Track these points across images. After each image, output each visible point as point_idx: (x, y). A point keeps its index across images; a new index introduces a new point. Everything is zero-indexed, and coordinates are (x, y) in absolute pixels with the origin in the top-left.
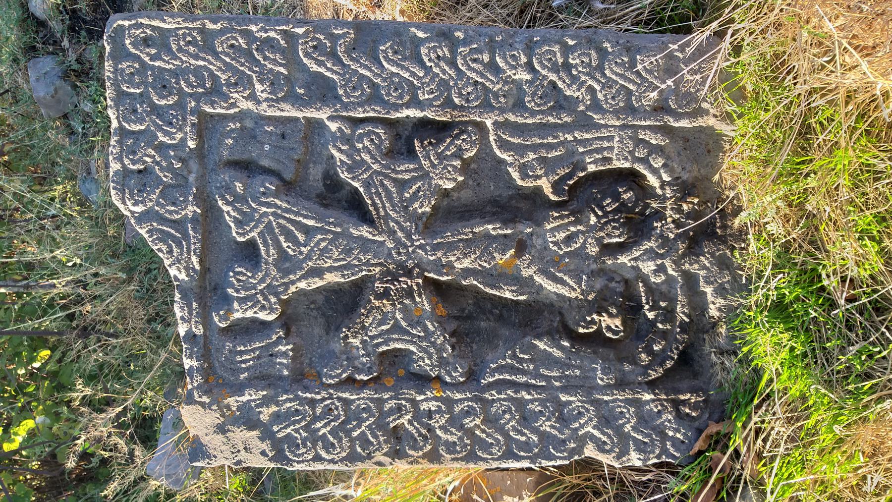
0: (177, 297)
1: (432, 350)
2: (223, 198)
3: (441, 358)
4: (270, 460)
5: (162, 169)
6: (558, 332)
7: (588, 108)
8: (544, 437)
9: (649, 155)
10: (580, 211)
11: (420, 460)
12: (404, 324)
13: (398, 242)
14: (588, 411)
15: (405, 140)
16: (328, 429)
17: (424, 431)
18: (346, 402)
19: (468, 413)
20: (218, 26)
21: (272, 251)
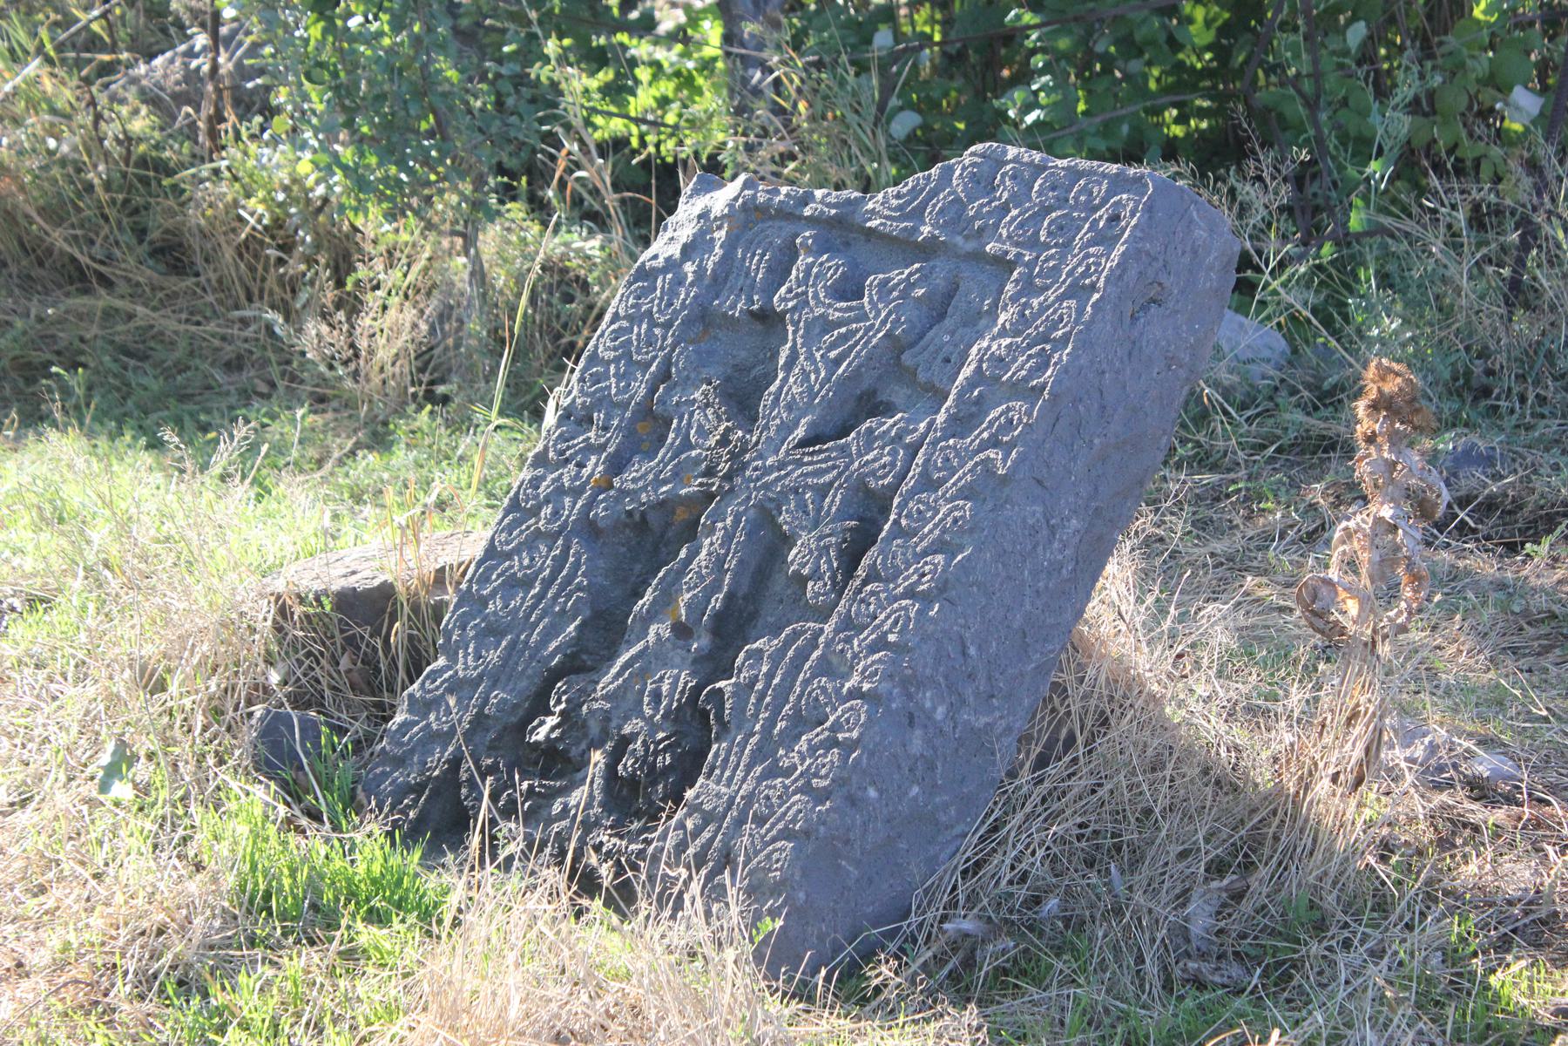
1: (641, 484)
2: (917, 271)
4: (643, 264)
5: (982, 206)
6: (574, 656)
8: (484, 602)
10: (676, 720)
13: (767, 471)
14: (475, 668)
19: (556, 514)
20: (1089, 309)
21: (837, 314)
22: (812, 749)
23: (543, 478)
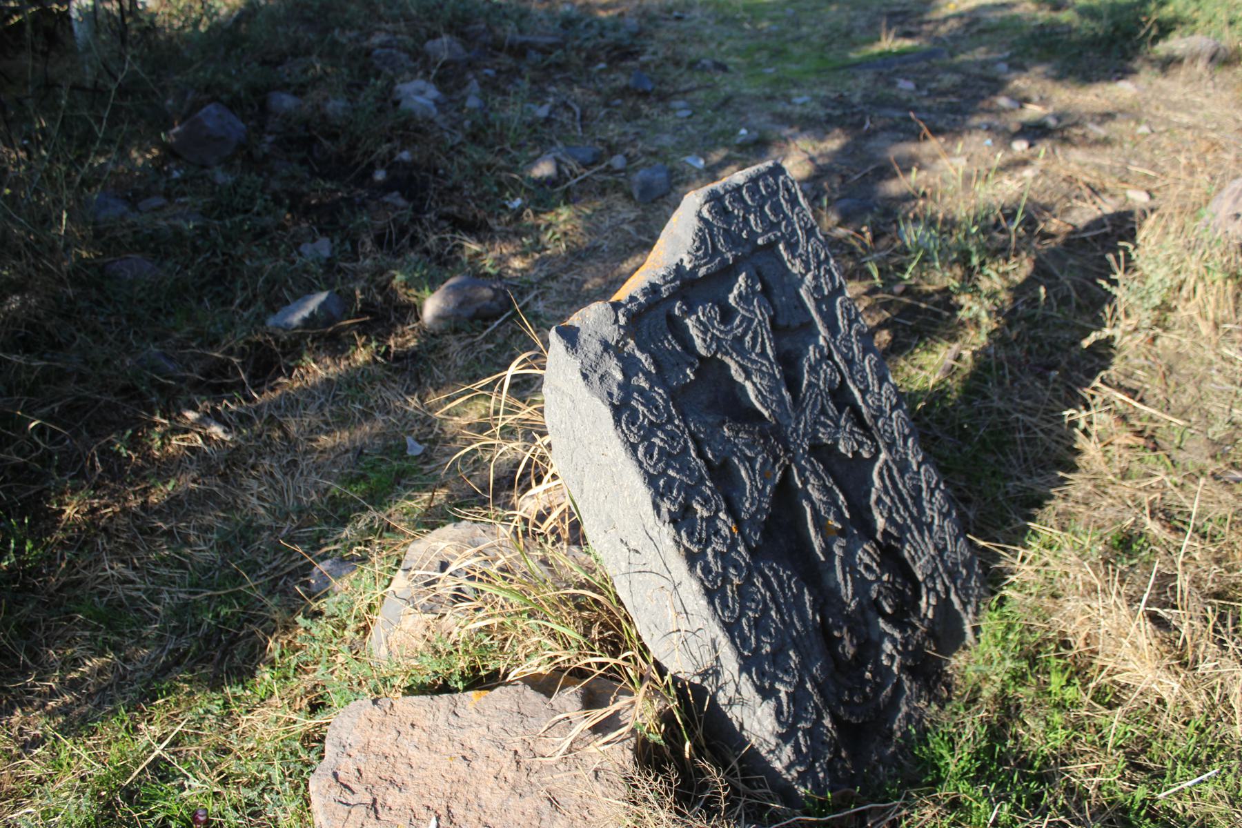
11: (682, 549)
12: (758, 466)
16: (661, 444)
17: (704, 535)
18: (685, 449)
19: (737, 566)
21: (740, 330)
23: (707, 563)
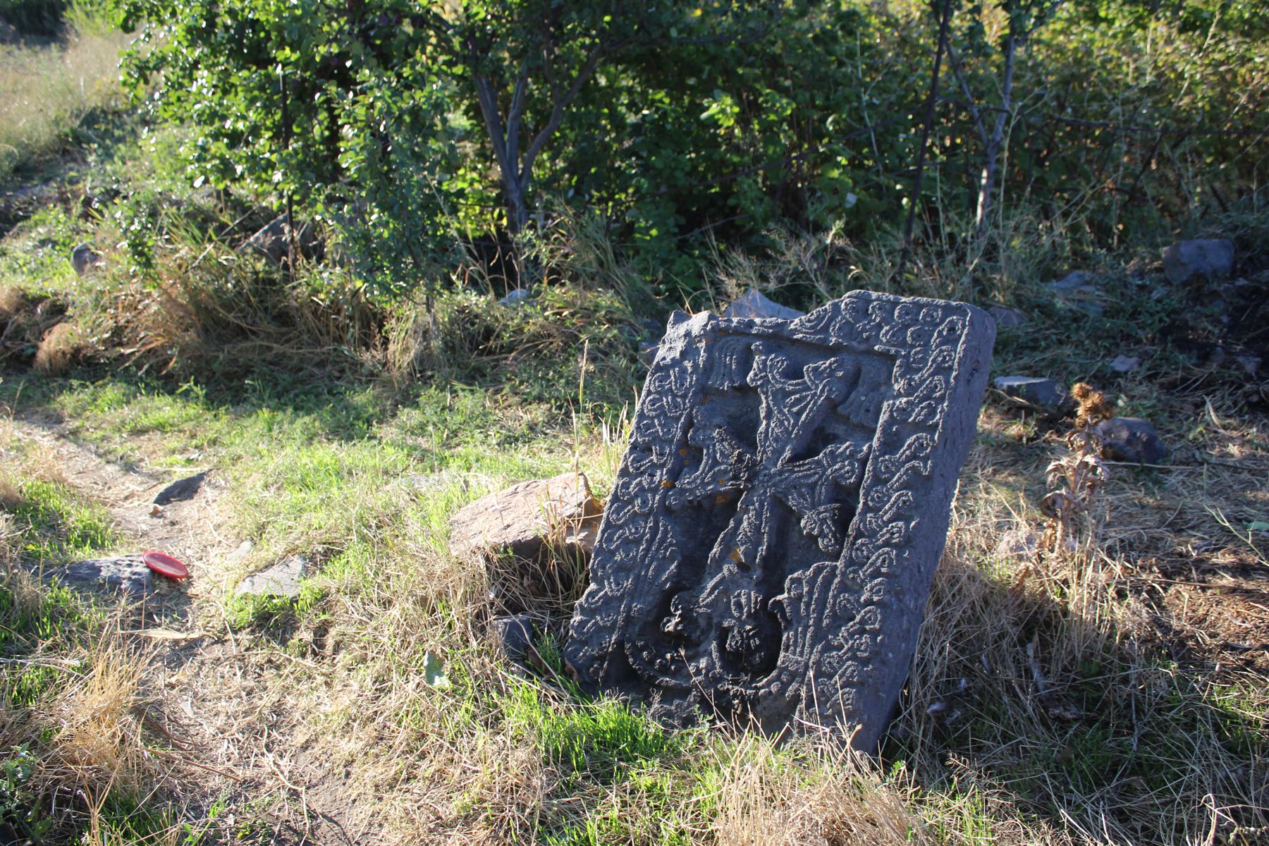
0: (780, 321)
3: (686, 490)
7: (828, 642)
8: (613, 553)
9: (782, 683)
15: (844, 499)
18: (679, 418)
19: (644, 502)
22: (851, 635)
23: (630, 483)
